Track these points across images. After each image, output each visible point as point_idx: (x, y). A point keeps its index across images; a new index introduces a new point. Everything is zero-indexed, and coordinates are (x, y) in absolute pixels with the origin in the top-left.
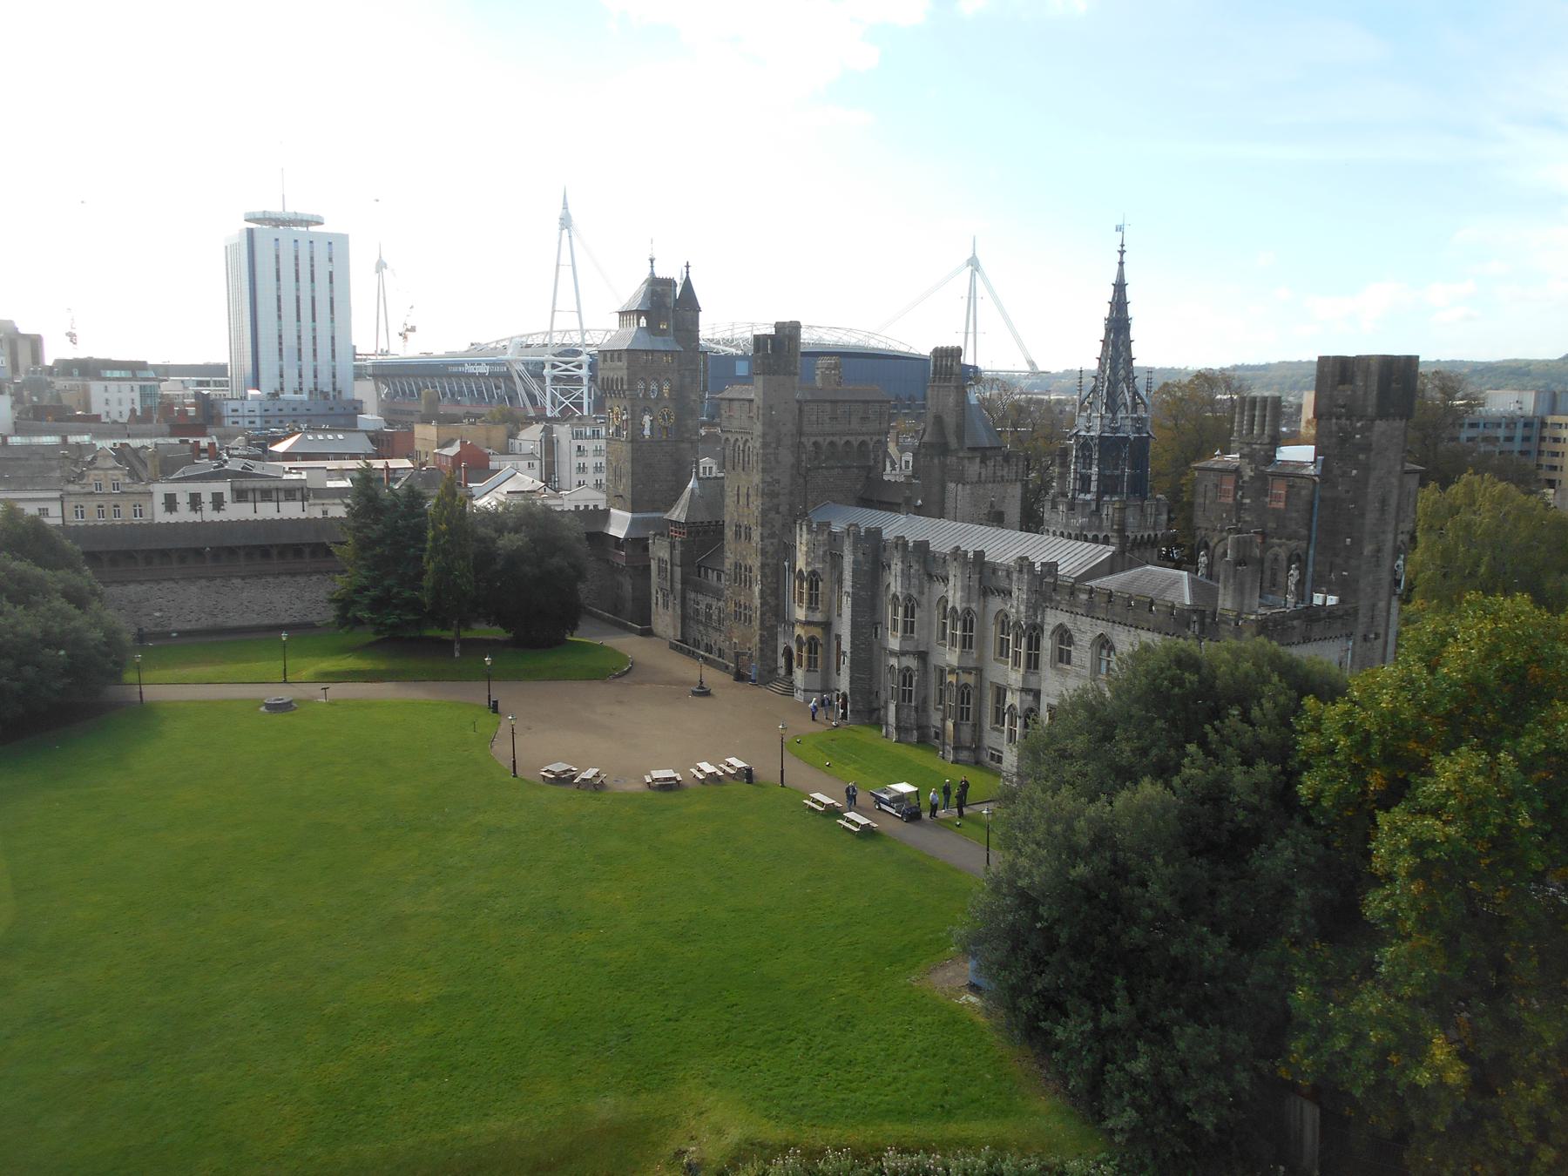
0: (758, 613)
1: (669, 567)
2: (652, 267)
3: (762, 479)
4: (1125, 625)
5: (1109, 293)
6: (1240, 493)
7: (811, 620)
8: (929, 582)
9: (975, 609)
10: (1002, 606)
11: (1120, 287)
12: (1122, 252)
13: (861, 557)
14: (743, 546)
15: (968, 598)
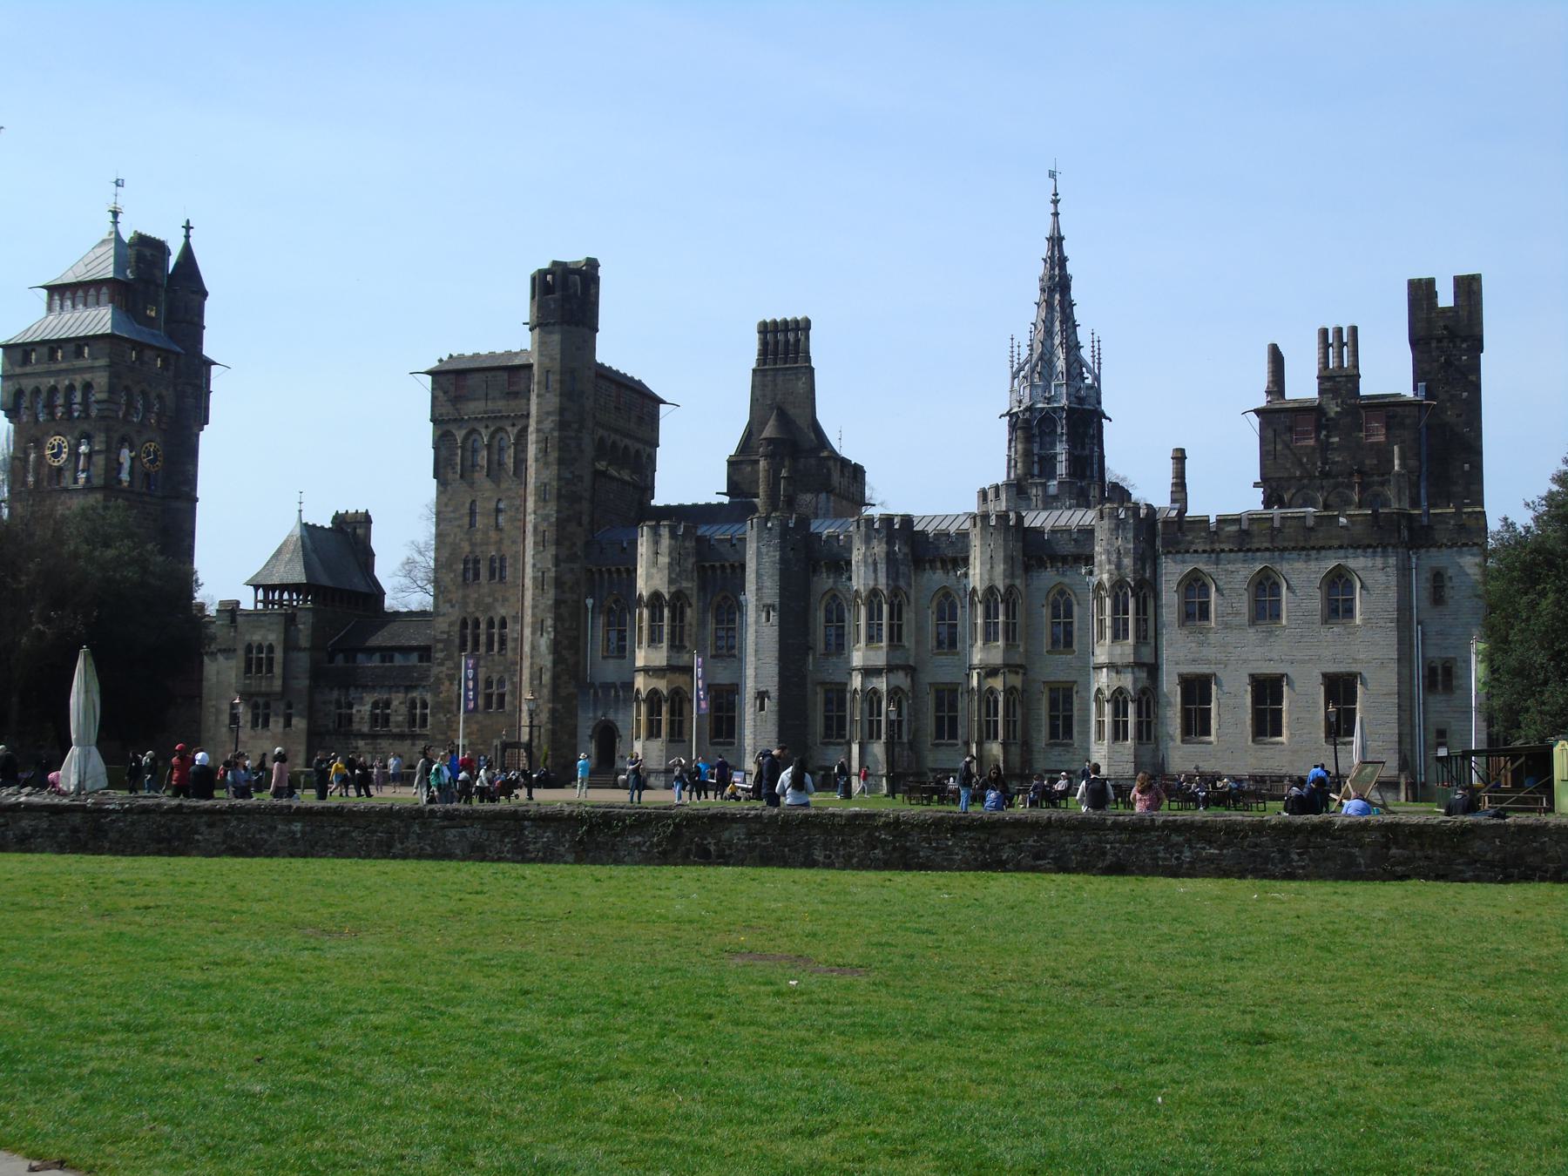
0: (546, 678)
1: (278, 655)
2: (115, 223)
3: (559, 475)
4: (1303, 549)
5: (1043, 249)
6: (1324, 433)
7: (675, 664)
8: (915, 575)
9: (1020, 587)
10: (1059, 579)
11: (1056, 241)
12: (1056, 202)
13: (791, 554)
14: (485, 590)
15: (1010, 574)
